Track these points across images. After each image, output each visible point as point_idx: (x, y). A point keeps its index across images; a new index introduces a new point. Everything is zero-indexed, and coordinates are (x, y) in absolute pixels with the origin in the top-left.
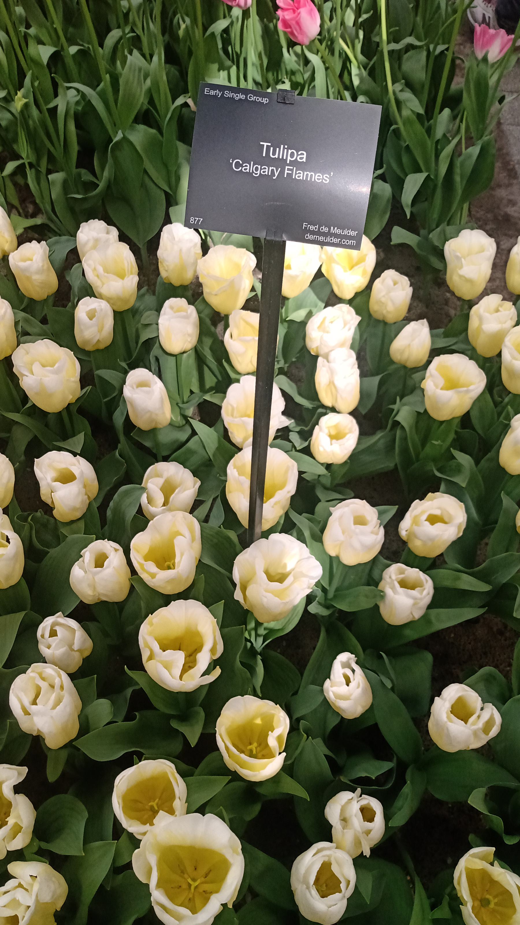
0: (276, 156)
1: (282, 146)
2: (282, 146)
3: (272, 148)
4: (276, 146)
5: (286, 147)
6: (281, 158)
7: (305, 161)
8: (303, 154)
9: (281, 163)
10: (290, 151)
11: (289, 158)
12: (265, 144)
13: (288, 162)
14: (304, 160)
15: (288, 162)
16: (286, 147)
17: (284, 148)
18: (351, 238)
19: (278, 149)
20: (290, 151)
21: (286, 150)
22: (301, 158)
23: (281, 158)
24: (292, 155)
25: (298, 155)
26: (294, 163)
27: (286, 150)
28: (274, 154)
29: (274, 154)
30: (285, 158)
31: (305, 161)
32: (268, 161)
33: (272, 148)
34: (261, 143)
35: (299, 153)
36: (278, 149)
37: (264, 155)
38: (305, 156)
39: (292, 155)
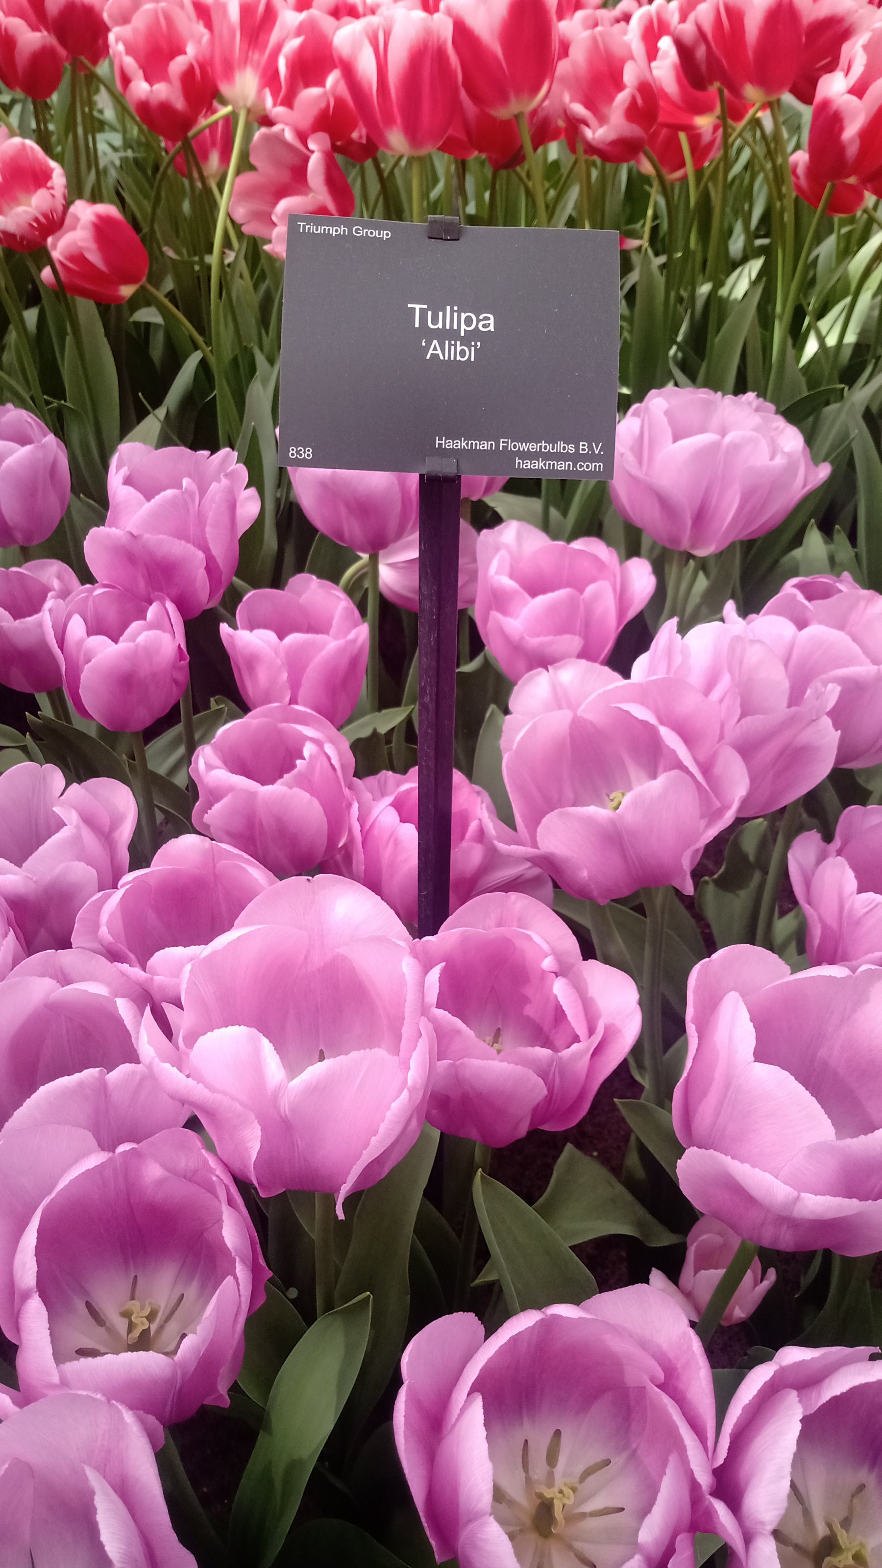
0: (440, 325)
1: (448, 308)
2: (448, 308)
3: (430, 313)
4: (436, 307)
5: (456, 308)
6: (448, 327)
7: (493, 330)
8: (489, 319)
10: (463, 316)
12: (418, 307)
13: (462, 334)
14: (492, 328)
15: (462, 334)
16: (456, 308)
17: (452, 311)
19: (441, 314)
20: (463, 316)
21: (456, 314)
22: (484, 326)
23: (448, 327)
24: (468, 321)
25: (478, 321)
26: (475, 334)
27: (456, 314)
29: (435, 321)
30: (455, 327)
31: (493, 330)
33: (430, 313)
34: (410, 306)
35: (481, 317)
36: (441, 314)
37: (417, 325)
38: (492, 321)
39: (468, 321)
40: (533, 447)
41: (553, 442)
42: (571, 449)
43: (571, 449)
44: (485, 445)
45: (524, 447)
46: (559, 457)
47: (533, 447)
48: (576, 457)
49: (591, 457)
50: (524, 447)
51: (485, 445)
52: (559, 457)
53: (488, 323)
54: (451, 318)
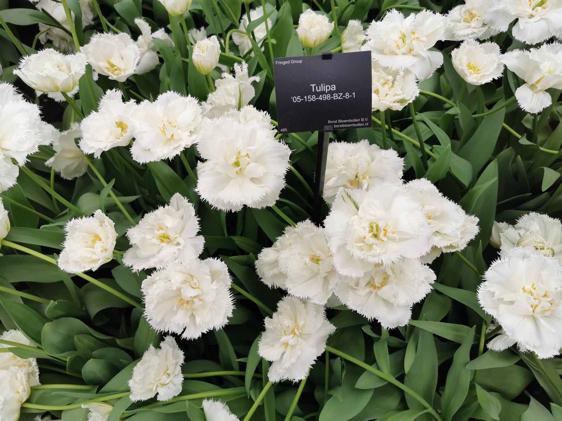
4: (318, 85)
9: (323, 93)
11: (327, 90)
12: (313, 85)
18: (365, 122)
24: (328, 88)
28: (318, 89)
29: (318, 89)
39: (328, 88)
46: (356, 123)
49: (365, 122)
53: (334, 88)
54: (323, 88)
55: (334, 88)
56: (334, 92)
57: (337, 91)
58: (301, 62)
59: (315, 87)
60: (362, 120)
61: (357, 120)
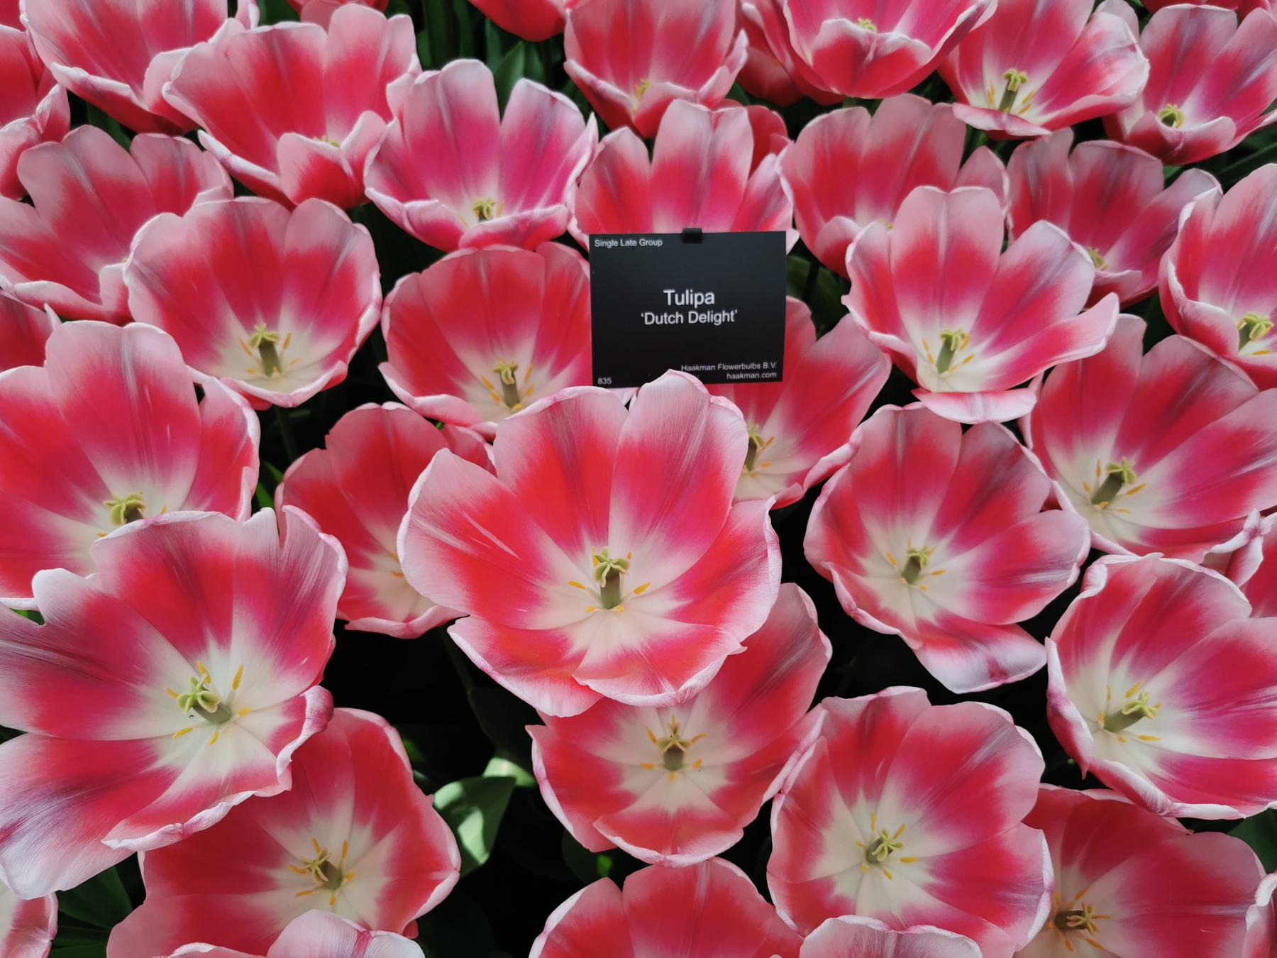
4: (680, 291)
11: (697, 303)
12: (669, 292)
24: (699, 298)
28: (680, 300)
29: (680, 300)
32: (673, 309)
38: (713, 298)
39: (699, 298)
40: (736, 367)
41: (748, 363)
42: (759, 366)
43: (759, 366)
44: (710, 368)
45: (731, 367)
46: (751, 371)
47: (736, 367)
48: (761, 371)
49: (770, 370)
50: (731, 367)
51: (710, 368)
52: (751, 371)
53: (710, 298)
54: (689, 298)
55: (710, 298)
56: (710, 307)
57: (716, 308)
58: (659, 243)
59: (673, 295)
60: (765, 365)
61: (753, 366)
